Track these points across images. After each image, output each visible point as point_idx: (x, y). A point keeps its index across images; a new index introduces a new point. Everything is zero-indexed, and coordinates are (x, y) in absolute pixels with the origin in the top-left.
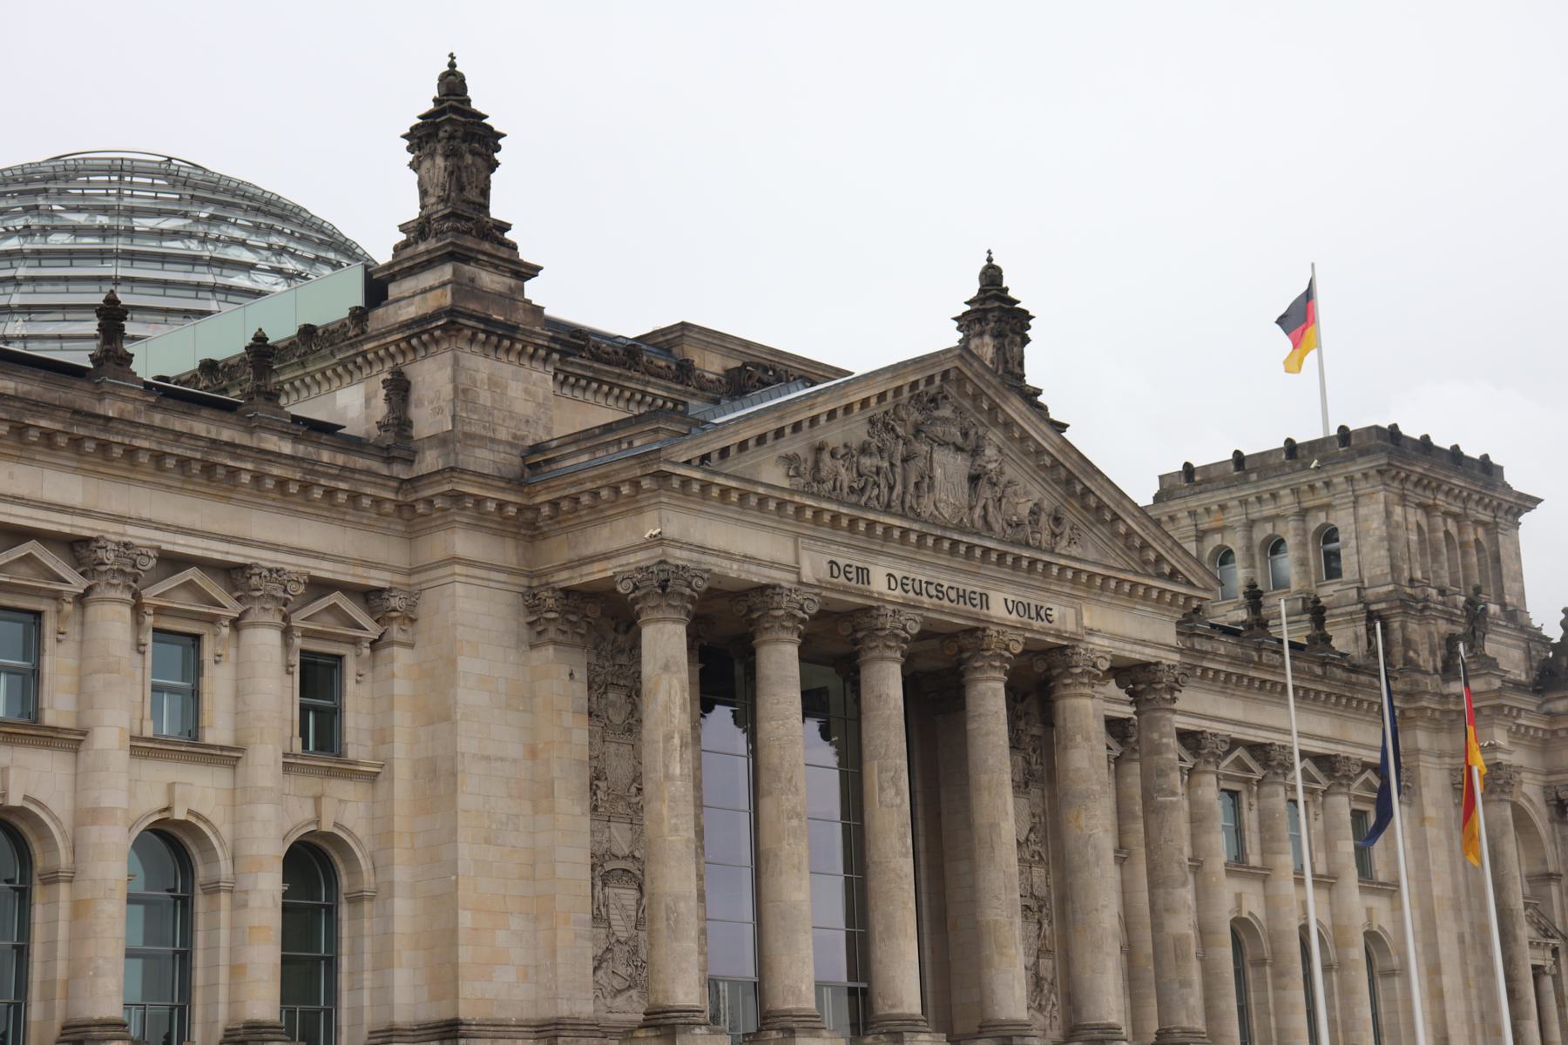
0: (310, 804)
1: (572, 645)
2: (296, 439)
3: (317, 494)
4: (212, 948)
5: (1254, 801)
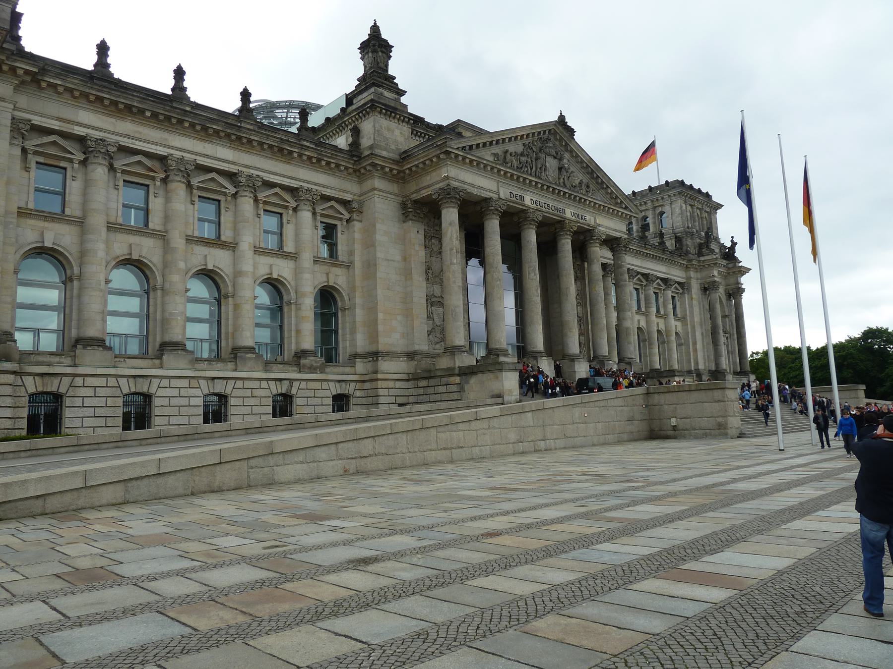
0: (325, 275)
1: (419, 221)
3: (324, 163)
4: (290, 324)
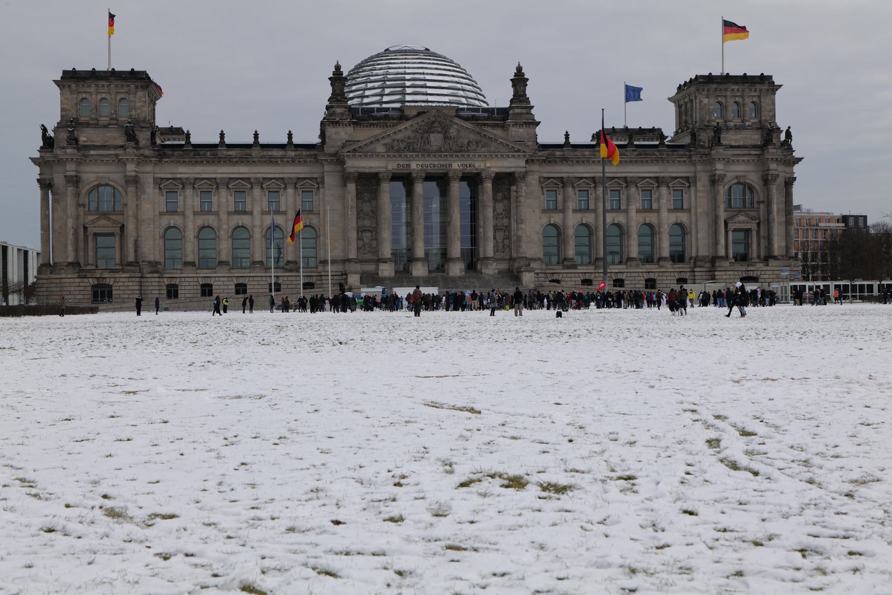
2: (295, 151)
3: (296, 162)
5: (625, 193)
